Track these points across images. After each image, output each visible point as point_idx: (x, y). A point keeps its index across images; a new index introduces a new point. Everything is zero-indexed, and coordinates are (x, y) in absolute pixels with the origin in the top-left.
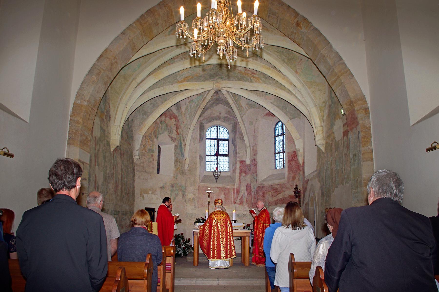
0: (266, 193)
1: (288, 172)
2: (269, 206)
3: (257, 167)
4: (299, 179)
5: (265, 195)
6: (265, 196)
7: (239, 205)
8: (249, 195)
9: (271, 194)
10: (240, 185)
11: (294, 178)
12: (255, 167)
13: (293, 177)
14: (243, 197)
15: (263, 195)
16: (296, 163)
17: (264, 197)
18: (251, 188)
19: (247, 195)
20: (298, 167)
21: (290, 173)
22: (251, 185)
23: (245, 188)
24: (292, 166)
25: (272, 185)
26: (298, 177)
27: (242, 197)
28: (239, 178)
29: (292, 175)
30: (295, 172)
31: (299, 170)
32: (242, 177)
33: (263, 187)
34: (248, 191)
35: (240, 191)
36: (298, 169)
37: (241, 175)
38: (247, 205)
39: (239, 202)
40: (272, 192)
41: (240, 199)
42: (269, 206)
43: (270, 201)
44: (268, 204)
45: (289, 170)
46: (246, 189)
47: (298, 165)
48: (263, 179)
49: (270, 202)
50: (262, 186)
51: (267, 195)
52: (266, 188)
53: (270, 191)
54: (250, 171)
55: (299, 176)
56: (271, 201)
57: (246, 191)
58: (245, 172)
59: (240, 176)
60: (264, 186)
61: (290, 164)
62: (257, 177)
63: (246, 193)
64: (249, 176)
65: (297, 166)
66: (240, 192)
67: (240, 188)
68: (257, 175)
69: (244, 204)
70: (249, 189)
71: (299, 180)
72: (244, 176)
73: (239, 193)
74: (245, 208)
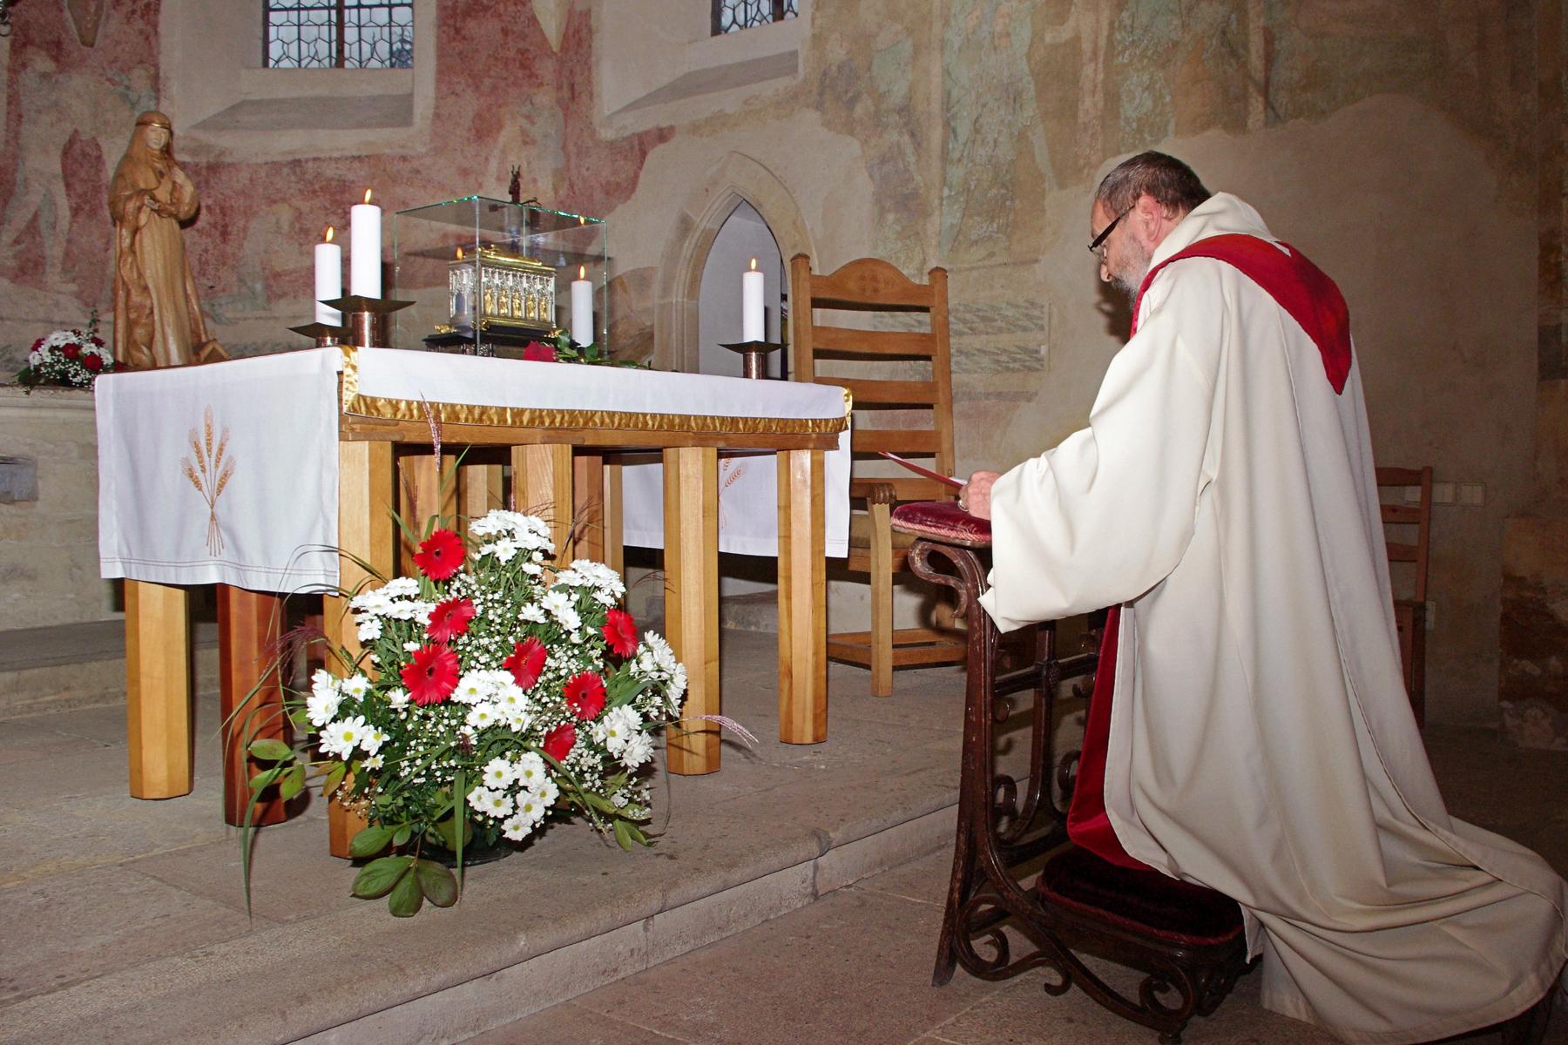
0: (249, 213)
1: (438, 89)
2: (269, 299)
3: (155, 26)
4: (523, 132)
5: (241, 223)
6: (233, 229)
7: (14, 279)
8: (82, 218)
9: (285, 214)
10: (17, 136)
11: (484, 130)
12: (139, 24)
13: (479, 116)
14: (42, 224)
15: (215, 226)
16: (505, 32)
17: (225, 234)
18: (98, 171)
19: (68, 213)
20: (525, 63)
21: (459, 89)
22: (98, 147)
23: (58, 168)
24: (477, 51)
25: (297, 163)
26: (523, 122)
27: (32, 227)
28: (11, 83)
29: (470, 104)
30: (494, 88)
31: (531, 76)
32: (29, 79)
33: (214, 168)
34: (79, 188)
35: (19, 177)
36: (520, 74)
37: (24, 66)
38: (73, 287)
39: (11, 263)
40: (305, 206)
41: (16, 242)
42: (269, 299)
43: (279, 269)
44: (259, 287)
45: (443, 72)
46: (65, 177)
47: (521, 45)
48: (200, 119)
49: (277, 276)
50: (203, 160)
51: (253, 224)
52: (244, 175)
53: (284, 200)
54: (92, 45)
55: (527, 117)
56: (292, 267)
57: (59, 189)
58: (56, 49)
59: (13, 71)
60: (228, 160)
61: (458, 31)
62: (158, 99)
63: (63, 204)
64: (77, 81)
65: (512, 54)
66: (19, 189)
67: (15, 157)
68: (156, 78)
69: (53, 276)
70: (83, 174)
71: (527, 140)
72: (45, 76)
73: (11, 193)
74: (57, 304)
